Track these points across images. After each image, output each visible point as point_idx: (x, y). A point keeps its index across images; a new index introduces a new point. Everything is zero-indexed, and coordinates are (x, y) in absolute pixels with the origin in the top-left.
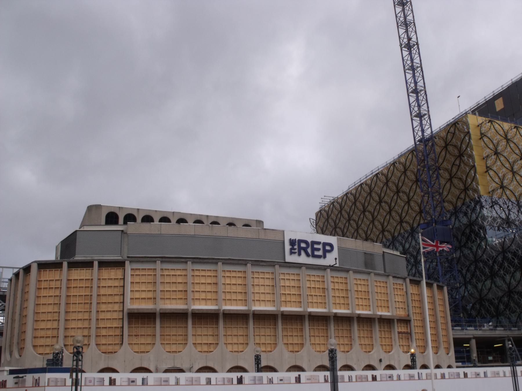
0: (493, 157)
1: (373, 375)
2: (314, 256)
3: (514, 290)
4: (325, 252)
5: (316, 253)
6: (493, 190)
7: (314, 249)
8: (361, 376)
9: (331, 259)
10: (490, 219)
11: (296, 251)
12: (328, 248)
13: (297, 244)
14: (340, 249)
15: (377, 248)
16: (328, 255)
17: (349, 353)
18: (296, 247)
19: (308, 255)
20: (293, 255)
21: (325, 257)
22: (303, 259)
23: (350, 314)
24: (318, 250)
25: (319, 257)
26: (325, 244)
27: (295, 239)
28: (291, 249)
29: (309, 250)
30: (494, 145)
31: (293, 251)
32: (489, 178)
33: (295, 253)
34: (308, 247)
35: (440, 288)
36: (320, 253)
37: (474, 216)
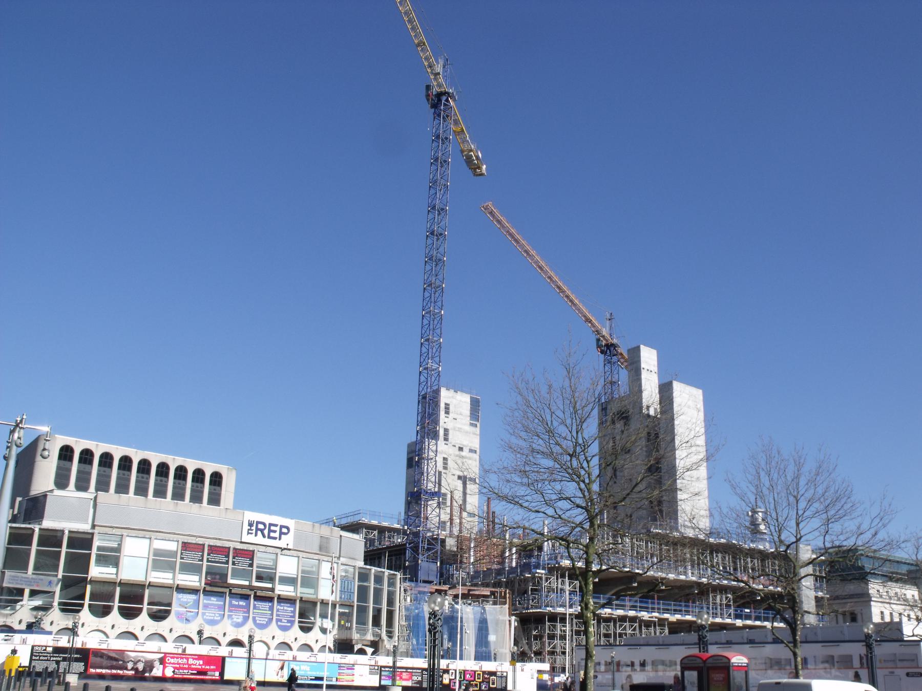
2: (269, 537)
5: (272, 534)
7: (270, 531)
11: (254, 532)
16: (283, 536)
18: (254, 528)
19: (264, 536)
21: (280, 539)
23: (293, 596)
24: (275, 532)
25: (275, 538)
26: (282, 527)
29: (266, 532)
31: (250, 531)
33: (252, 533)
36: (277, 535)
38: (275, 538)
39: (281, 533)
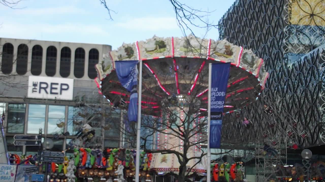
2: (51, 93)
5: (54, 91)
7: (52, 88)
11: (38, 90)
18: (38, 87)
19: (47, 92)
20: (34, 93)
21: (61, 93)
22: (43, 95)
24: (56, 89)
25: (57, 94)
26: (62, 85)
28: (33, 89)
29: (48, 90)
31: (34, 90)
33: (36, 91)
34: (47, 87)
36: (58, 91)
38: (57, 94)
39: (62, 89)
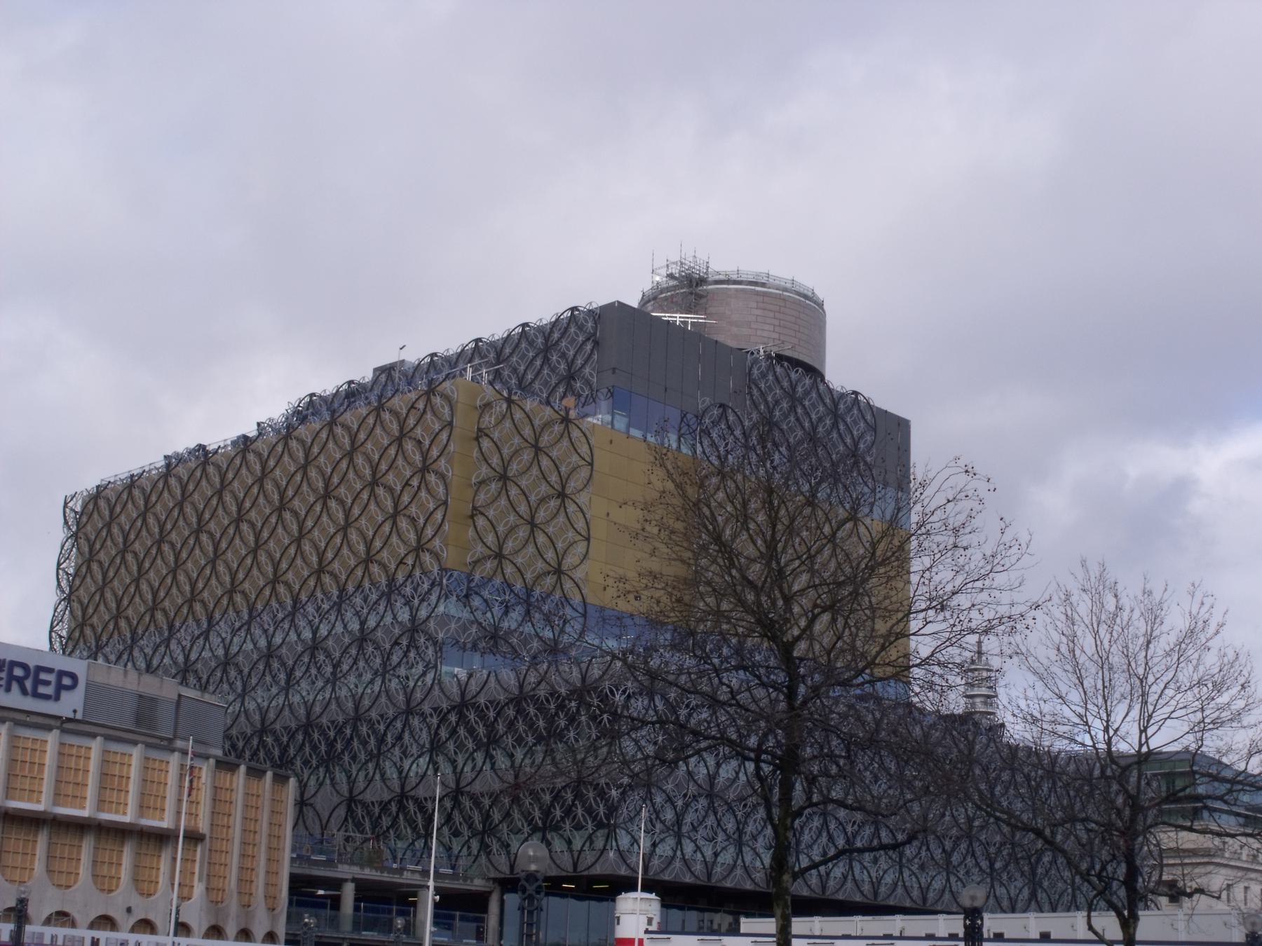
0: (493, 485)
1: (93, 938)
3: (468, 789)
4: (60, 687)
5: (42, 690)
6: (476, 562)
7: (37, 682)
8: (74, 937)
9: (71, 704)
10: (453, 626)
12: (64, 681)
13: (6, 669)
14: (89, 685)
15: (166, 689)
16: (64, 694)
17: (71, 889)
19: (24, 692)
21: (57, 698)
24: (47, 683)
25: (46, 697)
26: (62, 674)
27: (4, 660)
29: (28, 684)
30: (502, 459)
32: (471, 532)
34: (26, 677)
35: (280, 779)
37: (423, 613)
39: (60, 687)
